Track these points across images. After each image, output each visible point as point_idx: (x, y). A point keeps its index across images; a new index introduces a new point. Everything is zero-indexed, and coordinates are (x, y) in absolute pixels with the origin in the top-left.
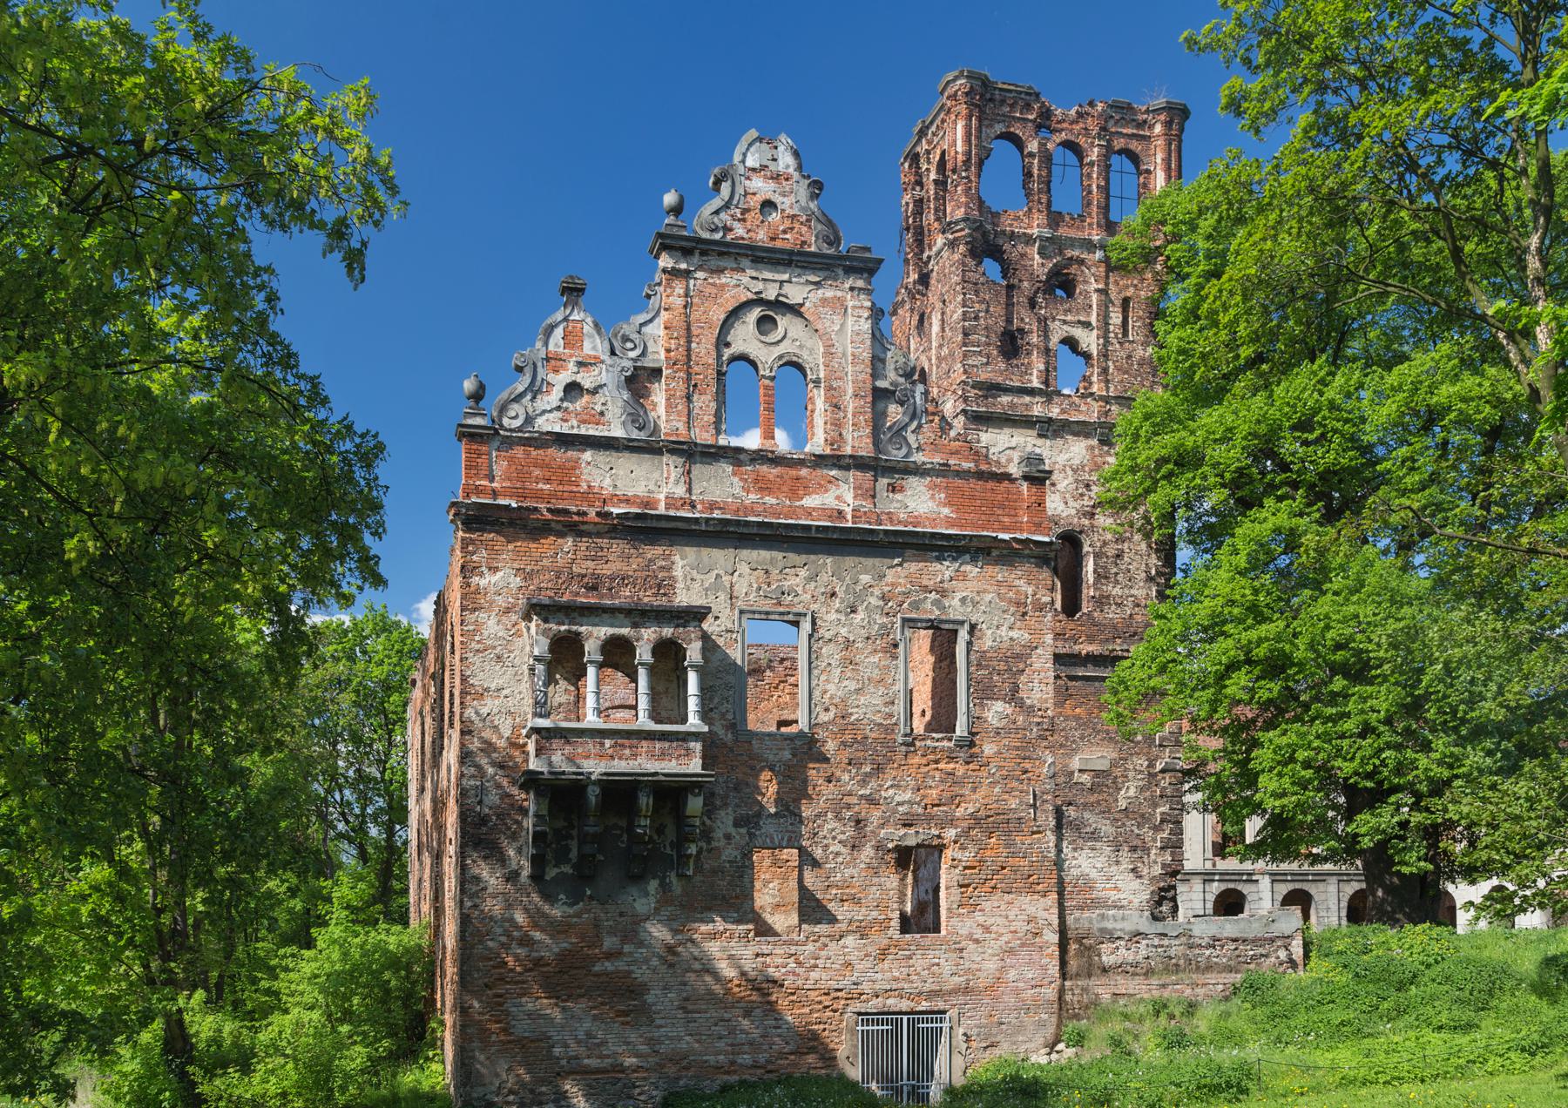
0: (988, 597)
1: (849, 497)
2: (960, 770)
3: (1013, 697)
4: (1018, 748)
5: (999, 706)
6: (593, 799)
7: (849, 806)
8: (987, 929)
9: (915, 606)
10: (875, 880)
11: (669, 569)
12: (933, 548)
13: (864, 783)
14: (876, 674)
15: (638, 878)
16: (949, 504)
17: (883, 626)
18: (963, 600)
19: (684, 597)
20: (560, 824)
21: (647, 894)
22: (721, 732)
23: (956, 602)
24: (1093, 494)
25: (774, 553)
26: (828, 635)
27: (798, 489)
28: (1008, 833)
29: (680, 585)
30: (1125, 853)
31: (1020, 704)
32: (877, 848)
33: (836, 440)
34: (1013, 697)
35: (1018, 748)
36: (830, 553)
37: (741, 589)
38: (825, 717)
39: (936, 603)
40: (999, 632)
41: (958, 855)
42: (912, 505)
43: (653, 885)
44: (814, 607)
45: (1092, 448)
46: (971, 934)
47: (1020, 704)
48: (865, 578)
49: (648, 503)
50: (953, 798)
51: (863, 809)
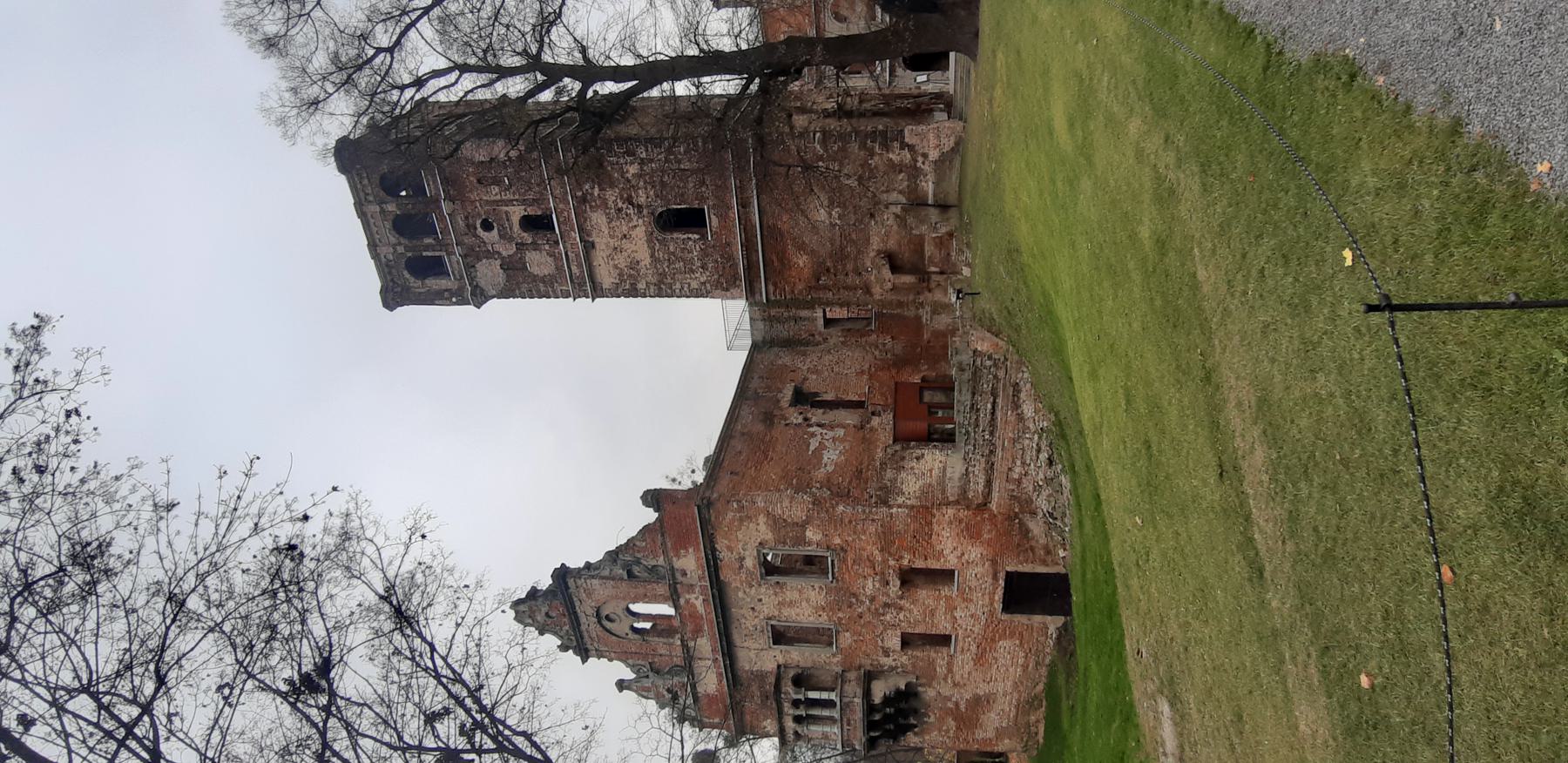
0: (740, 536)
2: (850, 557)
3: (803, 526)
4: (836, 526)
5: (809, 534)
12: (716, 565)
13: (862, 602)
16: (686, 549)
24: (624, 206)
27: (694, 616)
32: (901, 598)
35: (836, 526)
40: (761, 530)
45: (591, 207)
46: (958, 557)
48: (741, 594)
50: (869, 561)
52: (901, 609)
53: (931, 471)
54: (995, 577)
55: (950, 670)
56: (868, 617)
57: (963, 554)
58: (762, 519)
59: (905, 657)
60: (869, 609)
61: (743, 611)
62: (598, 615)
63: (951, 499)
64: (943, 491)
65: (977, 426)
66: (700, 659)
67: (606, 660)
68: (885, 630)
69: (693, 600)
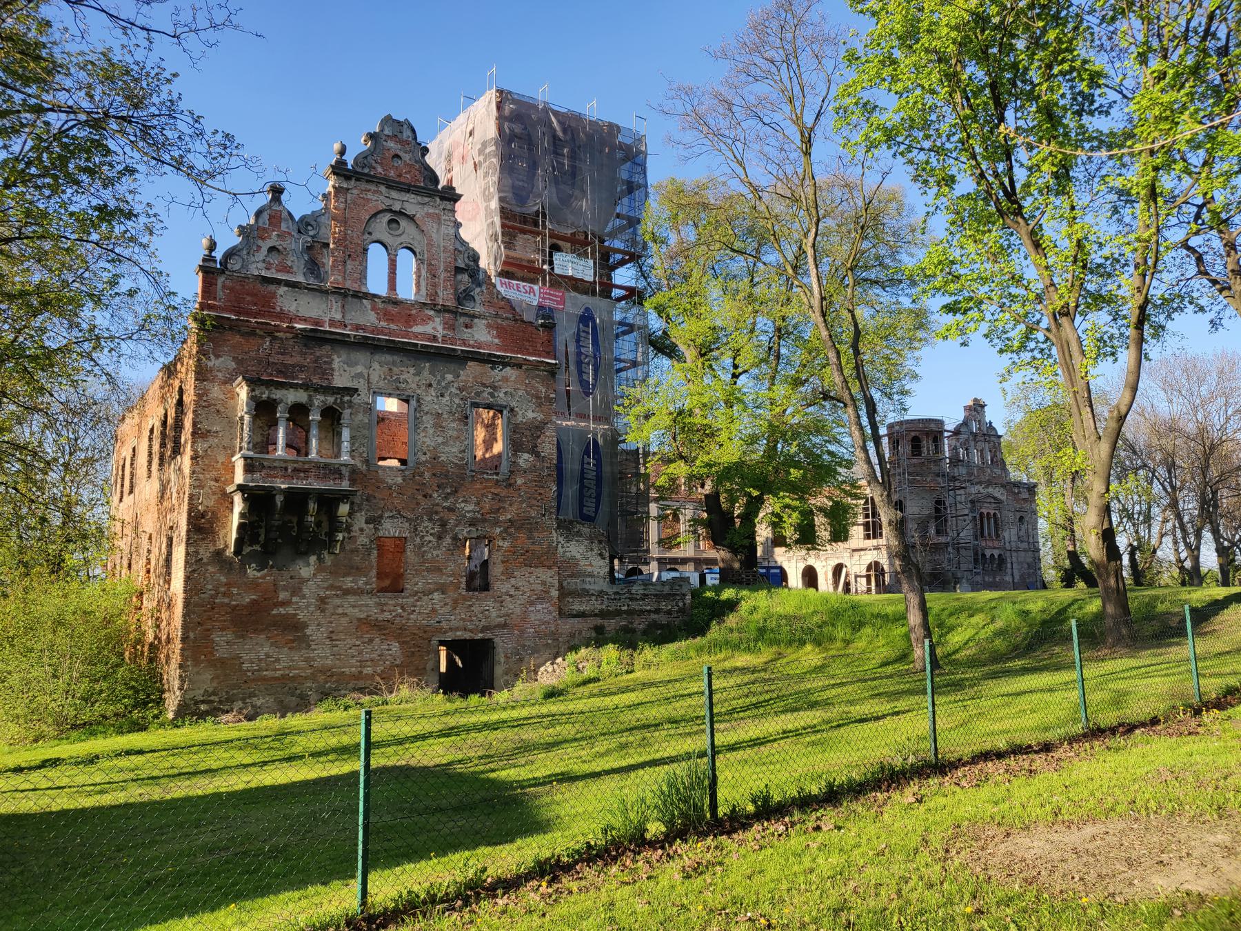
0: (520, 393)
1: (440, 328)
2: (504, 493)
3: (534, 451)
5: (526, 456)
6: (279, 504)
7: (437, 513)
8: (517, 589)
9: (478, 394)
10: (451, 558)
11: (330, 363)
13: (446, 498)
14: (455, 434)
15: (306, 554)
16: (498, 337)
17: (458, 406)
18: (506, 393)
19: (339, 381)
20: (255, 518)
21: (308, 565)
22: (359, 465)
23: (502, 395)
25: (396, 358)
26: (426, 409)
28: (530, 531)
29: (336, 373)
30: (595, 545)
31: (537, 455)
32: (455, 538)
33: (433, 295)
34: (534, 451)
36: (429, 361)
37: (374, 378)
38: (423, 458)
39: (490, 394)
41: (501, 544)
42: (476, 337)
43: (313, 559)
44: (419, 392)
47: (537, 455)
48: (449, 377)
49: (317, 322)
51: (445, 515)
52: (440, 538)
53: (591, 565)
54: (485, 629)
55: (347, 592)
56: (424, 503)
57: (511, 596)
58: (540, 417)
59: (366, 540)
60: (438, 505)
61: (426, 373)
62: (401, 213)
63: (565, 584)
64: (571, 576)
65: (631, 599)
66: (343, 306)
67: (462, 232)
68: (408, 520)
69: (431, 325)
